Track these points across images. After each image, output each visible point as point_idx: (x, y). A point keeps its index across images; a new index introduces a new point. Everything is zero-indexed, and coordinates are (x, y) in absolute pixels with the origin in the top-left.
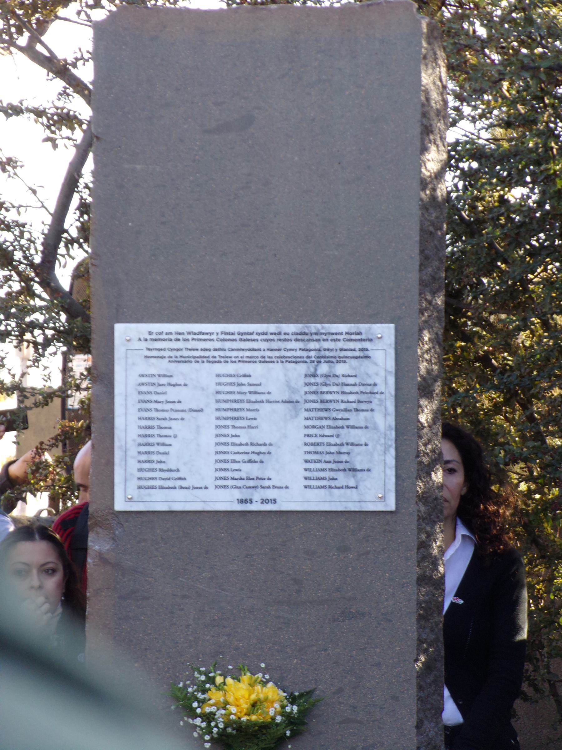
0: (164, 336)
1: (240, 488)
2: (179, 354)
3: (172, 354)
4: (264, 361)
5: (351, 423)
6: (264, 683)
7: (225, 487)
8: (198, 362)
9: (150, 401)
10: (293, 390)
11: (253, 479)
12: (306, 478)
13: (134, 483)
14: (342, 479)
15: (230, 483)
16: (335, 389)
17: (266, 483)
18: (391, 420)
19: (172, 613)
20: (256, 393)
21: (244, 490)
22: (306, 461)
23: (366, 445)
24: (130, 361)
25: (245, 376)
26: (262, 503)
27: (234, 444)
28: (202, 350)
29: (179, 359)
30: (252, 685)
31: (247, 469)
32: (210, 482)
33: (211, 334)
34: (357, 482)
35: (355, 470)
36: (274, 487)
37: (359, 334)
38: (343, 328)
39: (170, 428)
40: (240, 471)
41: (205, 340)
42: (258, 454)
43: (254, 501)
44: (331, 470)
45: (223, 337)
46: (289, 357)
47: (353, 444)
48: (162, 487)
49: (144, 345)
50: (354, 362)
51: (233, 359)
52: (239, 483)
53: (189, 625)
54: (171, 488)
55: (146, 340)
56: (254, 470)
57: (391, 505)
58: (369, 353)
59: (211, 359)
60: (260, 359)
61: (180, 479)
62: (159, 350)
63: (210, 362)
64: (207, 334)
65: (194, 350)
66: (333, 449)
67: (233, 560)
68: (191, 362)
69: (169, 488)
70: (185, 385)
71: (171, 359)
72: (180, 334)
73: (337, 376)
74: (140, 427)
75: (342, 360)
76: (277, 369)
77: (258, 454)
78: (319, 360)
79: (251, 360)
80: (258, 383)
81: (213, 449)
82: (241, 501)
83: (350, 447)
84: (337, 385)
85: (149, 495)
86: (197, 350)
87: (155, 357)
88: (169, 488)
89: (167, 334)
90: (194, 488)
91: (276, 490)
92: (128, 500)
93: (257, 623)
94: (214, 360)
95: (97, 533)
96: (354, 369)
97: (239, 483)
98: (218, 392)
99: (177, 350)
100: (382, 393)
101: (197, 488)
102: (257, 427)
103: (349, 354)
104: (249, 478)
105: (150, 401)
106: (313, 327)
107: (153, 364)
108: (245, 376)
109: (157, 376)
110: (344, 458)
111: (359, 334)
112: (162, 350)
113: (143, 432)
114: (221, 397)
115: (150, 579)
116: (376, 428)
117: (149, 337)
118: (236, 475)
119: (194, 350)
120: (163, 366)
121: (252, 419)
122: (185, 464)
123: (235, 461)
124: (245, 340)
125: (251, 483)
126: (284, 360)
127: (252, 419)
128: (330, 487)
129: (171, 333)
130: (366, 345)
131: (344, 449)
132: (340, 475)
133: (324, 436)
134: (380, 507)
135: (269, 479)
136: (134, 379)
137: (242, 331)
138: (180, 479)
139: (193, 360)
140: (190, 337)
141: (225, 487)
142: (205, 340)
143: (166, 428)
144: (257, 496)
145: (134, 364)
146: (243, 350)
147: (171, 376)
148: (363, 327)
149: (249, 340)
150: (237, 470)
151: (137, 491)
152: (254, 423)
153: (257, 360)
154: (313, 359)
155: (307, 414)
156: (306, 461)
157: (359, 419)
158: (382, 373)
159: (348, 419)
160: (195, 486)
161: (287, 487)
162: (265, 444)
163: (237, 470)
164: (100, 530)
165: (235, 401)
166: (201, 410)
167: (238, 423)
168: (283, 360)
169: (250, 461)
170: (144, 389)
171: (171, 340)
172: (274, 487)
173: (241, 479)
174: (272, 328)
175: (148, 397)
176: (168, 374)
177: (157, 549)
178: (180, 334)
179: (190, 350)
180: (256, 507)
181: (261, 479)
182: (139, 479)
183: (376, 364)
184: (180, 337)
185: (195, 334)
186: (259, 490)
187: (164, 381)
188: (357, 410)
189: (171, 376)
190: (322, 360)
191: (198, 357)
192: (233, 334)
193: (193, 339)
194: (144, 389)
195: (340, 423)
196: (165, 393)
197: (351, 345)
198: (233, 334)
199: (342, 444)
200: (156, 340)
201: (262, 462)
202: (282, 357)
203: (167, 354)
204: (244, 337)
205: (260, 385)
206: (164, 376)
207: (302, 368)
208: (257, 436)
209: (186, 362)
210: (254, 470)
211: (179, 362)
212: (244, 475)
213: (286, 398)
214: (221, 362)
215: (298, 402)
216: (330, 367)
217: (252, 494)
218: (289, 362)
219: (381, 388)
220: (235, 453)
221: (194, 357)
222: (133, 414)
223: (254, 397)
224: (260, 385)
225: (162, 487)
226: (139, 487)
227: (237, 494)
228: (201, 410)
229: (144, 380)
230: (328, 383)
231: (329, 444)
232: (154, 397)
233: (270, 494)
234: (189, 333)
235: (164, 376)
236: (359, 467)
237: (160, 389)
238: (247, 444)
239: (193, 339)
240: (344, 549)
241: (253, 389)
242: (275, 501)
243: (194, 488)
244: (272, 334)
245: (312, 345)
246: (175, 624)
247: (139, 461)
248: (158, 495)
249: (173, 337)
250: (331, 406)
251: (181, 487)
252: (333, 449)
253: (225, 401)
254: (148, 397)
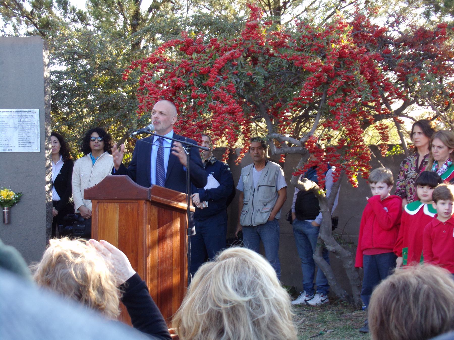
4: (8, 118)
6: (10, 191)
10: (15, 125)
14: (27, 145)
18: (39, 131)
30: (7, 191)
31: (5, 143)
38: (27, 110)
50: (30, 118)
56: (7, 143)
57: (39, 151)
66: (25, 138)
75: (27, 118)
76: (11, 120)
78: (21, 117)
79: (5, 118)
106: (20, 110)
130: (32, 114)
131: (28, 138)
132: (27, 144)
134: (37, 151)
144: (7, 149)
148: (31, 110)
157: (32, 131)
167: (3, 132)
168: (13, 117)
174: (10, 110)
180: (7, 151)
197: (29, 114)
207: (17, 120)
208: (7, 135)
210: (7, 143)
227: (3, 148)
233: (11, 148)
240: (28, 161)
242: (11, 150)
245: (20, 114)
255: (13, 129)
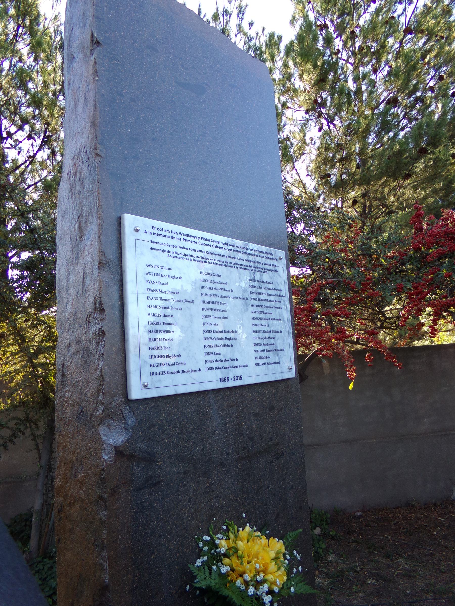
0: (163, 233)
1: (220, 369)
2: (175, 250)
3: (171, 249)
5: (273, 316)
7: (211, 369)
8: (188, 259)
9: (155, 290)
11: (228, 360)
12: (256, 358)
13: (147, 370)
15: (214, 365)
16: (264, 291)
17: (236, 363)
19: (178, 491)
20: (224, 290)
21: (223, 370)
22: (255, 345)
23: (281, 332)
24: (139, 251)
25: (218, 275)
26: (234, 380)
27: (215, 332)
28: (190, 249)
29: (175, 255)
32: (202, 365)
33: (196, 237)
34: (279, 359)
35: (277, 350)
36: (240, 366)
37: (271, 254)
39: (172, 316)
40: (220, 354)
41: (191, 242)
42: (229, 339)
43: (229, 379)
44: (267, 351)
45: (202, 241)
46: (241, 265)
47: (275, 332)
48: (169, 373)
49: (149, 237)
51: (210, 261)
52: (220, 365)
53: (190, 499)
54: (176, 373)
55: (151, 233)
58: (277, 269)
59: (196, 259)
60: (225, 263)
61: (182, 363)
62: (161, 244)
63: (196, 260)
64: (193, 237)
65: (185, 248)
66: (267, 335)
67: (215, 431)
68: (183, 258)
69: (174, 373)
70: (181, 278)
71: (170, 254)
72: (175, 233)
73: (264, 282)
74: (149, 315)
77: (229, 339)
80: (225, 282)
81: (202, 335)
82: (223, 380)
83: (274, 334)
84: (265, 288)
85: (160, 381)
86: (187, 249)
87: (158, 250)
88: (174, 373)
89: (165, 231)
90: (192, 371)
91: (241, 368)
92: (143, 388)
93: (233, 480)
94: (198, 259)
95: (109, 426)
96: (272, 278)
97: (220, 365)
98: (202, 287)
99: (174, 246)
100: (284, 297)
101: (194, 371)
102: (227, 318)
103: (268, 267)
104: (226, 360)
105: (155, 290)
107: (157, 256)
108: (218, 275)
109: (160, 267)
110: (272, 341)
111: (271, 254)
112: (162, 244)
113: (152, 319)
114: (205, 291)
115: (160, 463)
116: (284, 321)
117: (153, 231)
118: (218, 357)
119: (185, 248)
120: (163, 259)
121: (224, 311)
122: (184, 349)
123: (216, 346)
124: (216, 247)
125: (227, 364)
126: (238, 266)
127: (224, 311)
128: (268, 364)
129: (168, 231)
131: (272, 335)
132: (271, 354)
133: (261, 325)
135: (237, 360)
136: (142, 269)
137: (214, 240)
138: (182, 363)
139: (185, 257)
140: (182, 237)
141: (211, 369)
142: (191, 242)
143: (169, 316)
144: (232, 374)
145: (141, 253)
146: (215, 254)
147: (170, 269)
148: (272, 250)
149: (218, 247)
150: (218, 354)
151: (150, 377)
152: (225, 314)
153: (224, 264)
154: (252, 268)
155: (252, 309)
156: (255, 345)
158: (283, 283)
159: (271, 313)
160: (193, 369)
161: (247, 366)
162: (232, 332)
163: (218, 354)
164: (111, 422)
165: (213, 296)
166: (192, 302)
167: (217, 314)
169: (225, 346)
170: (151, 278)
171: (169, 237)
172: (240, 366)
173: (221, 361)
175: (154, 286)
176: (168, 267)
177: (163, 432)
178: (175, 233)
179: (182, 248)
181: (233, 360)
182: (151, 365)
183: (280, 276)
184: (175, 235)
185: (185, 235)
186: (232, 369)
187: (165, 272)
188: (275, 308)
189: (170, 269)
190: (257, 270)
191: (188, 256)
192: (208, 240)
193: (184, 239)
194: (151, 278)
195: (268, 316)
196: (167, 284)
197: (268, 261)
198: (208, 240)
199: (270, 332)
200: (158, 235)
201: (232, 346)
202: (237, 264)
203: (166, 248)
204: (215, 244)
205: (226, 284)
206: (165, 268)
209: (180, 258)
211: (175, 257)
212: (221, 357)
213: (240, 296)
214: (203, 262)
215: (247, 299)
216: (261, 275)
217: (228, 373)
218: (241, 268)
219: (283, 293)
220: (216, 339)
221: (186, 255)
222: (143, 302)
223: (224, 294)
224: (226, 284)
225: (169, 373)
226: (152, 374)
227: (219, 374)
228: (192, 302)
229: (151, 270)
230: (261, 287)
231: (265, 332)
232: (159, 287)
233: (238, 372)
234: (181, 234)
235: (165, 268)
236: (279, 349)
237: (163, 280)
238: (222, 332)
239: (184, 239)
241: (222, 286)
242: (241, 378)
243: (192, 371)
244: (230, 245)
246: (181, 501)
247: (150, 348)
248: (166, 380)
249: (170, 234)
250: (264, 303)
251: (183, 372)
252: (267, 335)
253: (208, 295)
254: (154, 286)
255: (239, 302)
